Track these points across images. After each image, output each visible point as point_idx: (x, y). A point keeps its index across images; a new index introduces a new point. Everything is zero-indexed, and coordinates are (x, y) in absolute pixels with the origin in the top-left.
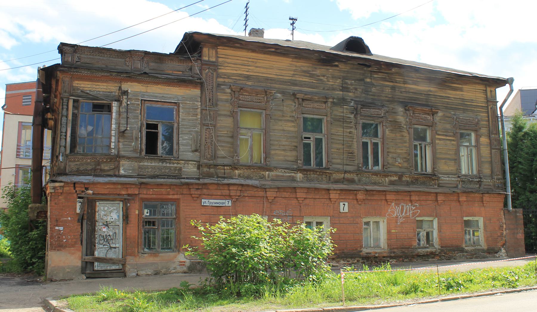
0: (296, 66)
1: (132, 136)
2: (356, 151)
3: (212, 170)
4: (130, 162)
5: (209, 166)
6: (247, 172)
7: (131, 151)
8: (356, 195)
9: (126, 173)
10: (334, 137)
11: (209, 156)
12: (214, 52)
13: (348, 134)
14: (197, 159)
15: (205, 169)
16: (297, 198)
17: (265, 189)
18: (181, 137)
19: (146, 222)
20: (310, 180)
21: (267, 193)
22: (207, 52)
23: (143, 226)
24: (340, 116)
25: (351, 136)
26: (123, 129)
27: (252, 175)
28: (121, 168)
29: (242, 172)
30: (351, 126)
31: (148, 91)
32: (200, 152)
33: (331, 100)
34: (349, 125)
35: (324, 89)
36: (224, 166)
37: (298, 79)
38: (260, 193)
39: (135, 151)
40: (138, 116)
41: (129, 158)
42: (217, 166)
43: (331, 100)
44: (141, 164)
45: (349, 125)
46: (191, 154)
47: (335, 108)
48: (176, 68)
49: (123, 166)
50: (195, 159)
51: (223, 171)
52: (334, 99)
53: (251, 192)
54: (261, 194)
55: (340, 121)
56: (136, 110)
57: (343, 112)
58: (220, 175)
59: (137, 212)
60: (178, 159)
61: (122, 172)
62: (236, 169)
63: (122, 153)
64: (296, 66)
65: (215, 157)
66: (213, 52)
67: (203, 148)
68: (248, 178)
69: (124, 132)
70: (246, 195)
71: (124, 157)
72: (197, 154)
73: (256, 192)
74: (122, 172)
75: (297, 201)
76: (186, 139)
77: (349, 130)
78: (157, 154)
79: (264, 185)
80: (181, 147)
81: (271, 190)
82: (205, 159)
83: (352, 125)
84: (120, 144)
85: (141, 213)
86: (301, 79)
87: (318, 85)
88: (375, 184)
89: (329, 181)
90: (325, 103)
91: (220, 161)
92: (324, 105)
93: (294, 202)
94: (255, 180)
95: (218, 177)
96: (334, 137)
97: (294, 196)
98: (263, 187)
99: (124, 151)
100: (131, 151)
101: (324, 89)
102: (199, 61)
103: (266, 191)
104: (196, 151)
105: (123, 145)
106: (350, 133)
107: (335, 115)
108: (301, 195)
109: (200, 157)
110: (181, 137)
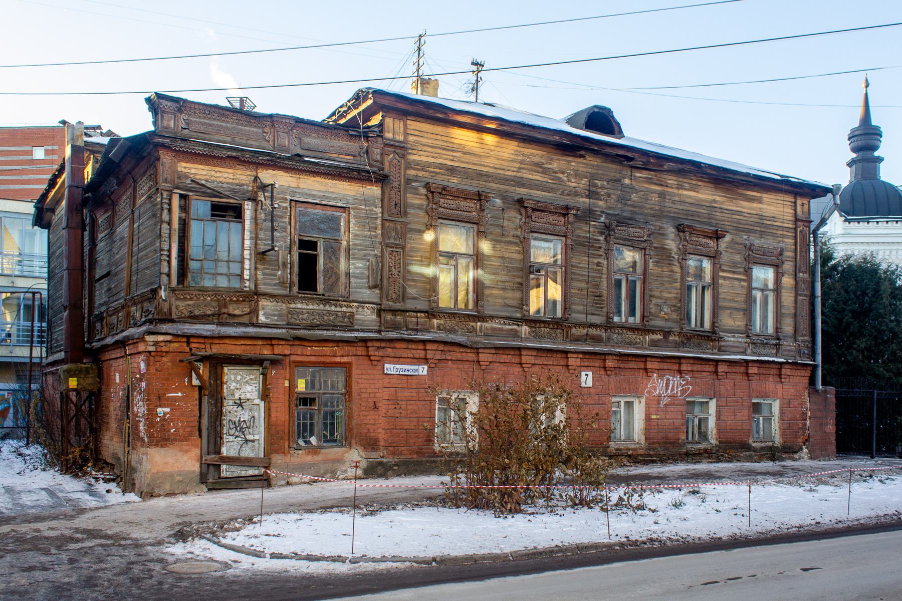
0: (523, 155)
1: (278, 261)
2: (605, 293)
3: (399, 318)
4: (275, 303)
5: (394, 312)
6: (450, 323)
7: (275, 285)
8: (605, 360)
9: (268, 321)
10: (575, 270)
11: (394, 296)
12: (402, 125)
13: (595, 267)
14: (376, 300)
15: (389, 317)
16: (521, 364)
17: (478, 349)
18: (353, 264)
19: (300, 399)
20: (539, 337)
21: (480, 355)
22: (391, 125)
23: (296, 406)
24: (584, 237)
25: (599, 270)
26: (262, 247)
27: (456, 328)
28: (261, 313)
29: (442, 322)
30: (600, 253)
31: (302, 186)
32: (381, 289)
33: (573, 212)
34: (597, 252)
35: (562, 194)
36: (417, 312)
37: (525, 176)
38: (470, 355)
39: (282, 284)
40: (286, 228)
41: (272, 296)
42: (408, 311)
43: (573, 212)
44: (293, 306)
45: (597, 252)
46: (368, 291)
47: (579, 225)
48: (343, 150)
49: (263, 309)
50: (375, 300)
51: (414, 320)
52: (578, 210)
53: (456, 354)
54: (471, 356)
55: (585, 246)
56: (282, 217)
57: (589, 232)
58: (411, 326)
59: (287, 384)
60: (348, 300)
61: (262, 319)
62: (435, 317)
63: (262, 288)
64: (523, 155)
65: (404, 297)
66: (399, 125)
67: (385, 281)
68: (452, 331)
69: (264, 253)
70: (449, 358)
71: (265, 295)
72: (377, 291)
73: (464, 354)
74: (262, 319)
75: (521, 369)
76: (360, 268)
77: (596, 261)
78: (316, 290)
79: (476, 343)
80: (352, 280)
81: (486, 351)
82: (388, 300)
83: (601, 252)
84: (259, 273)
85: (292, 386)
86: (530, 177)
87: (554, 186)
88: (631, 344)
89: (568, 338)
90: (564, 215)
91: (410, 305)
92: (562, 219)
93: (517, 370)
94: (462, 335)
95: (408, 329)
96: (575, 270)
97: (517, 360)
98: (475, 346)
99: (265, 284)
100: (275, 285)
101: (562, 194)
102: (380, 139)
103: (478, 353)
104: (375, 287)
105: (264, 274)
106: (598, 264)
107: (580, 237)
108: (527, 359)
109: (381, 298)
110: (353, 264)
